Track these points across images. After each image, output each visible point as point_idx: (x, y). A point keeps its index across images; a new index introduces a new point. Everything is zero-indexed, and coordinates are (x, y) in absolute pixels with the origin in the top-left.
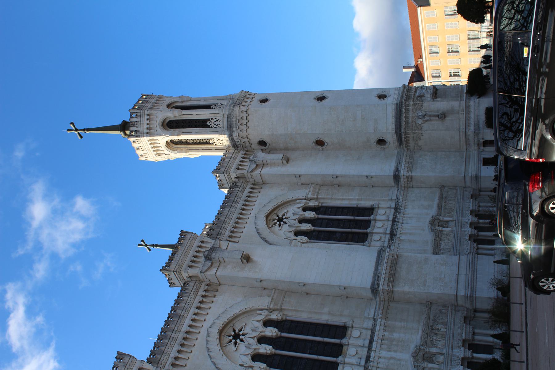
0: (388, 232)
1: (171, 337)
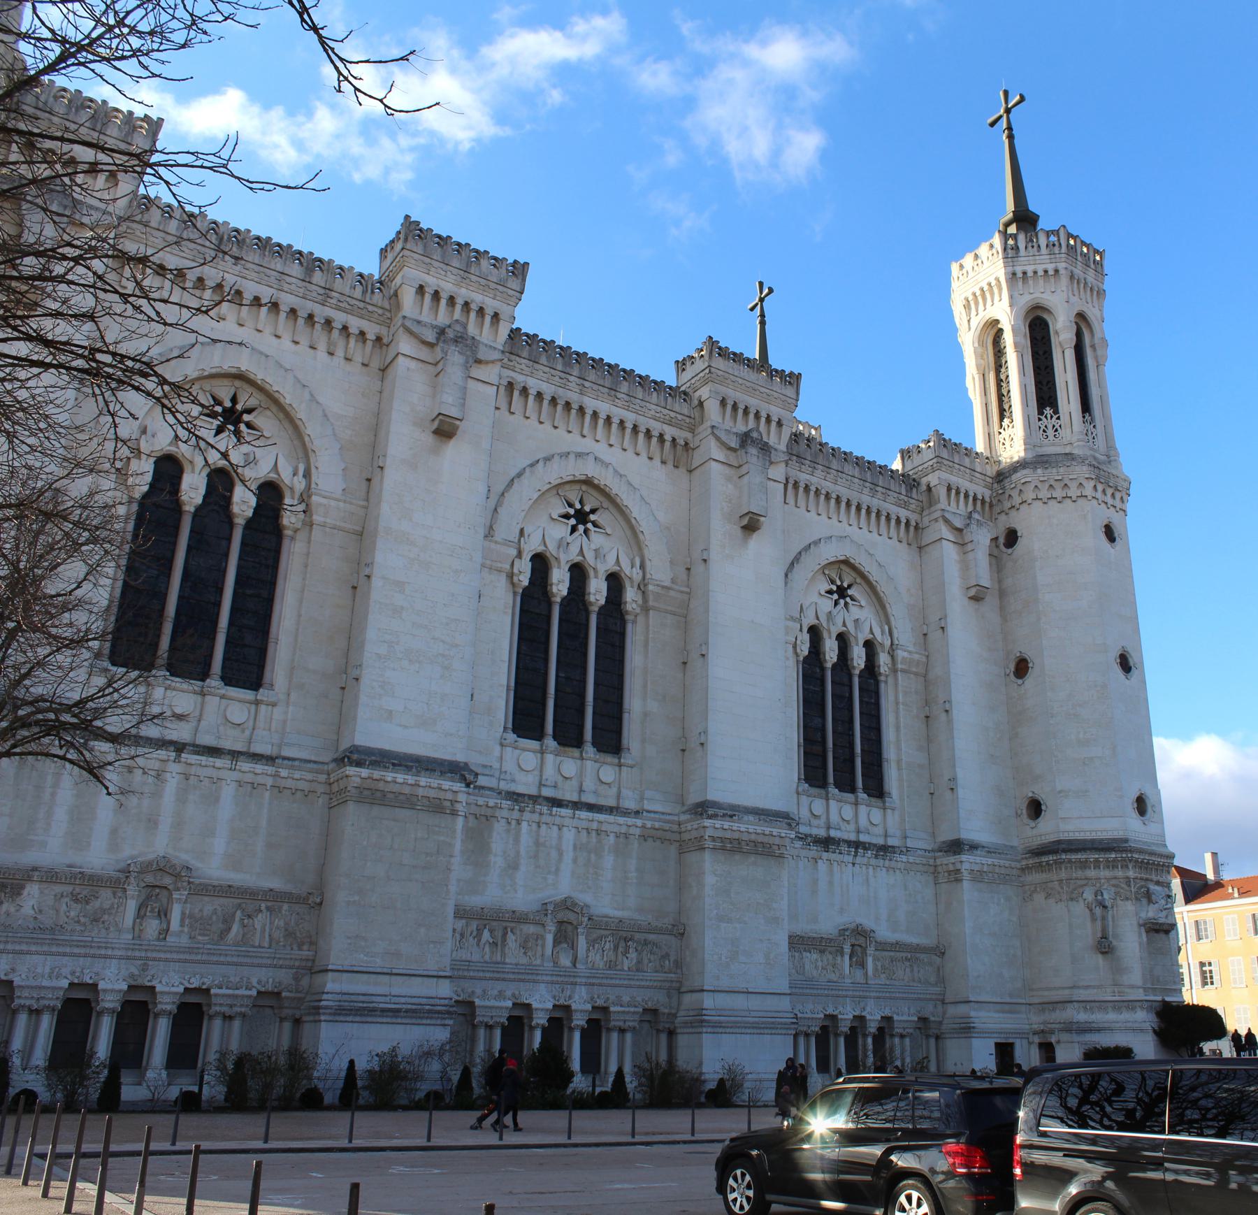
0: (833, 833)
1: (568, 376)
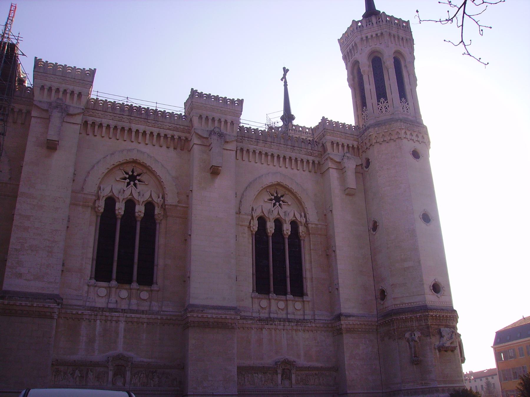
0: (272, 316)
1: (123, 116)
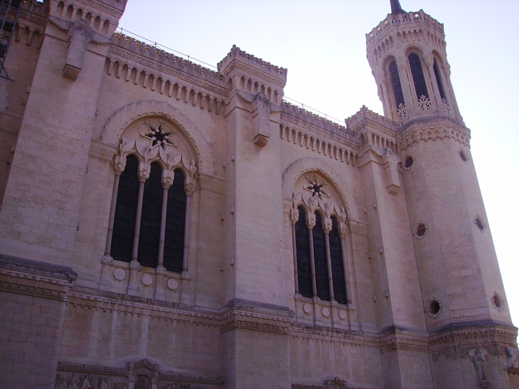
0: (318, 323)
1: (152, 61)
